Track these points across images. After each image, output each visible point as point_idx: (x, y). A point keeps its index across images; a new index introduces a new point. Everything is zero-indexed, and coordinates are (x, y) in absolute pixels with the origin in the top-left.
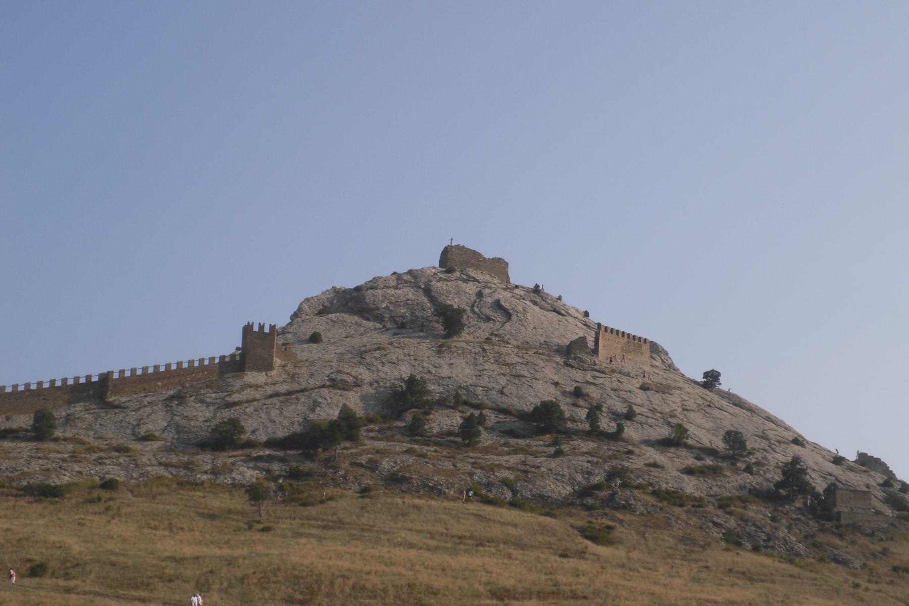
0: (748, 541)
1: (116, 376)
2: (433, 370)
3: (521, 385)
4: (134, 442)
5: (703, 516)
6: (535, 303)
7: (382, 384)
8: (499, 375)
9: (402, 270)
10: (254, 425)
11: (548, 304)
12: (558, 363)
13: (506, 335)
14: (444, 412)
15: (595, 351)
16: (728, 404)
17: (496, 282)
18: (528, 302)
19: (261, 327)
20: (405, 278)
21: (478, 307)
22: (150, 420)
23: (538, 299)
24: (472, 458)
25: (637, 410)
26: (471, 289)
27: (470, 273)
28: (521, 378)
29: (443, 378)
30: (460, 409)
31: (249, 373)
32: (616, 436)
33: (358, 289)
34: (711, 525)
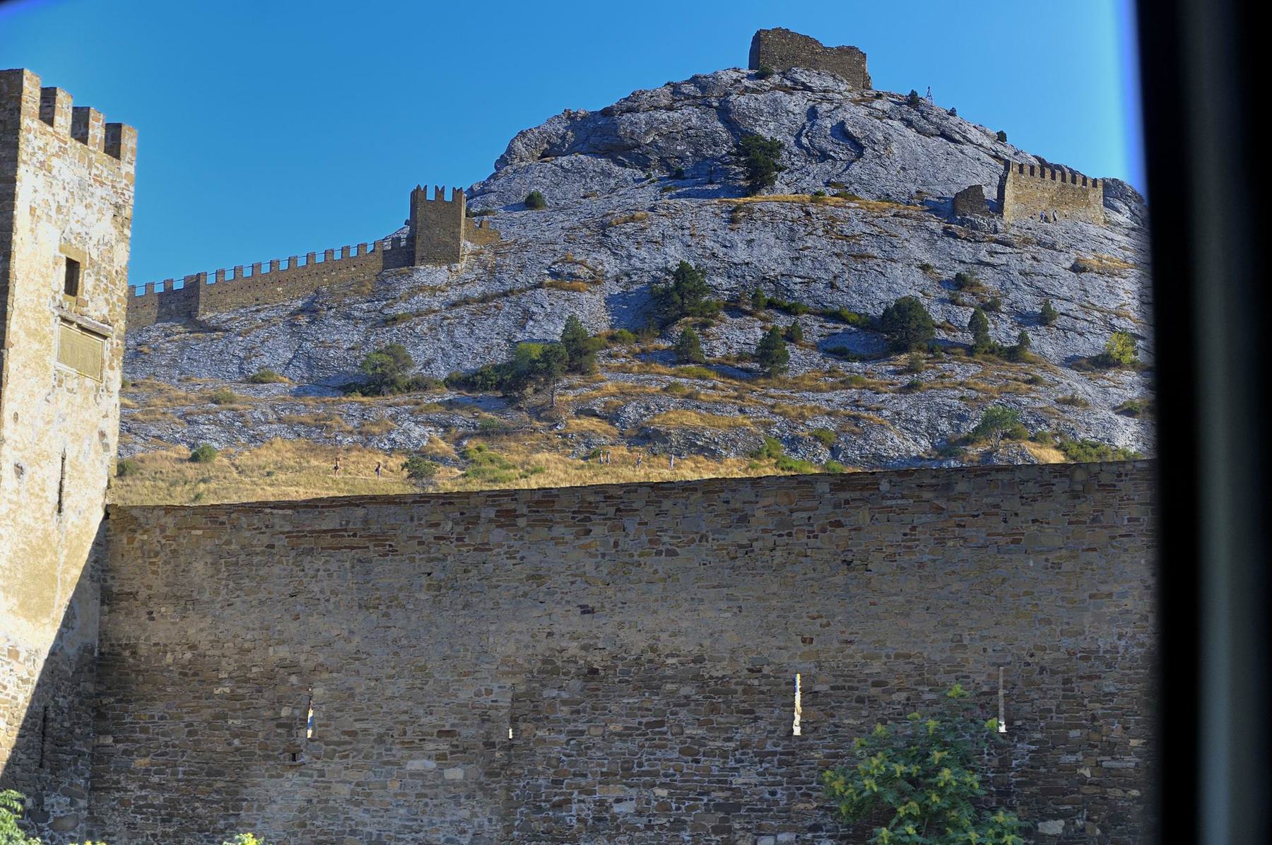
1: (211, 280)
2: (720, 252)
4: (243, 385)
6: (909, 124)
7: (635, 278)
11: (932, 123)
12: (932, 232)
13: (851, 184)
14: (735, 320)
15: (998, 207)
17: (842, 89)
18: (896, 123)
19: (440, 193)
23: (914, 116)
24: (772, 397)
25: (1059, 307)
26: (797, 104)
27: (797, 76)
28: (866, 260)
29: (735, 264)
30: (763, 314)
31: (422, 267)
32: (1013, 355)
33: (607, 112)
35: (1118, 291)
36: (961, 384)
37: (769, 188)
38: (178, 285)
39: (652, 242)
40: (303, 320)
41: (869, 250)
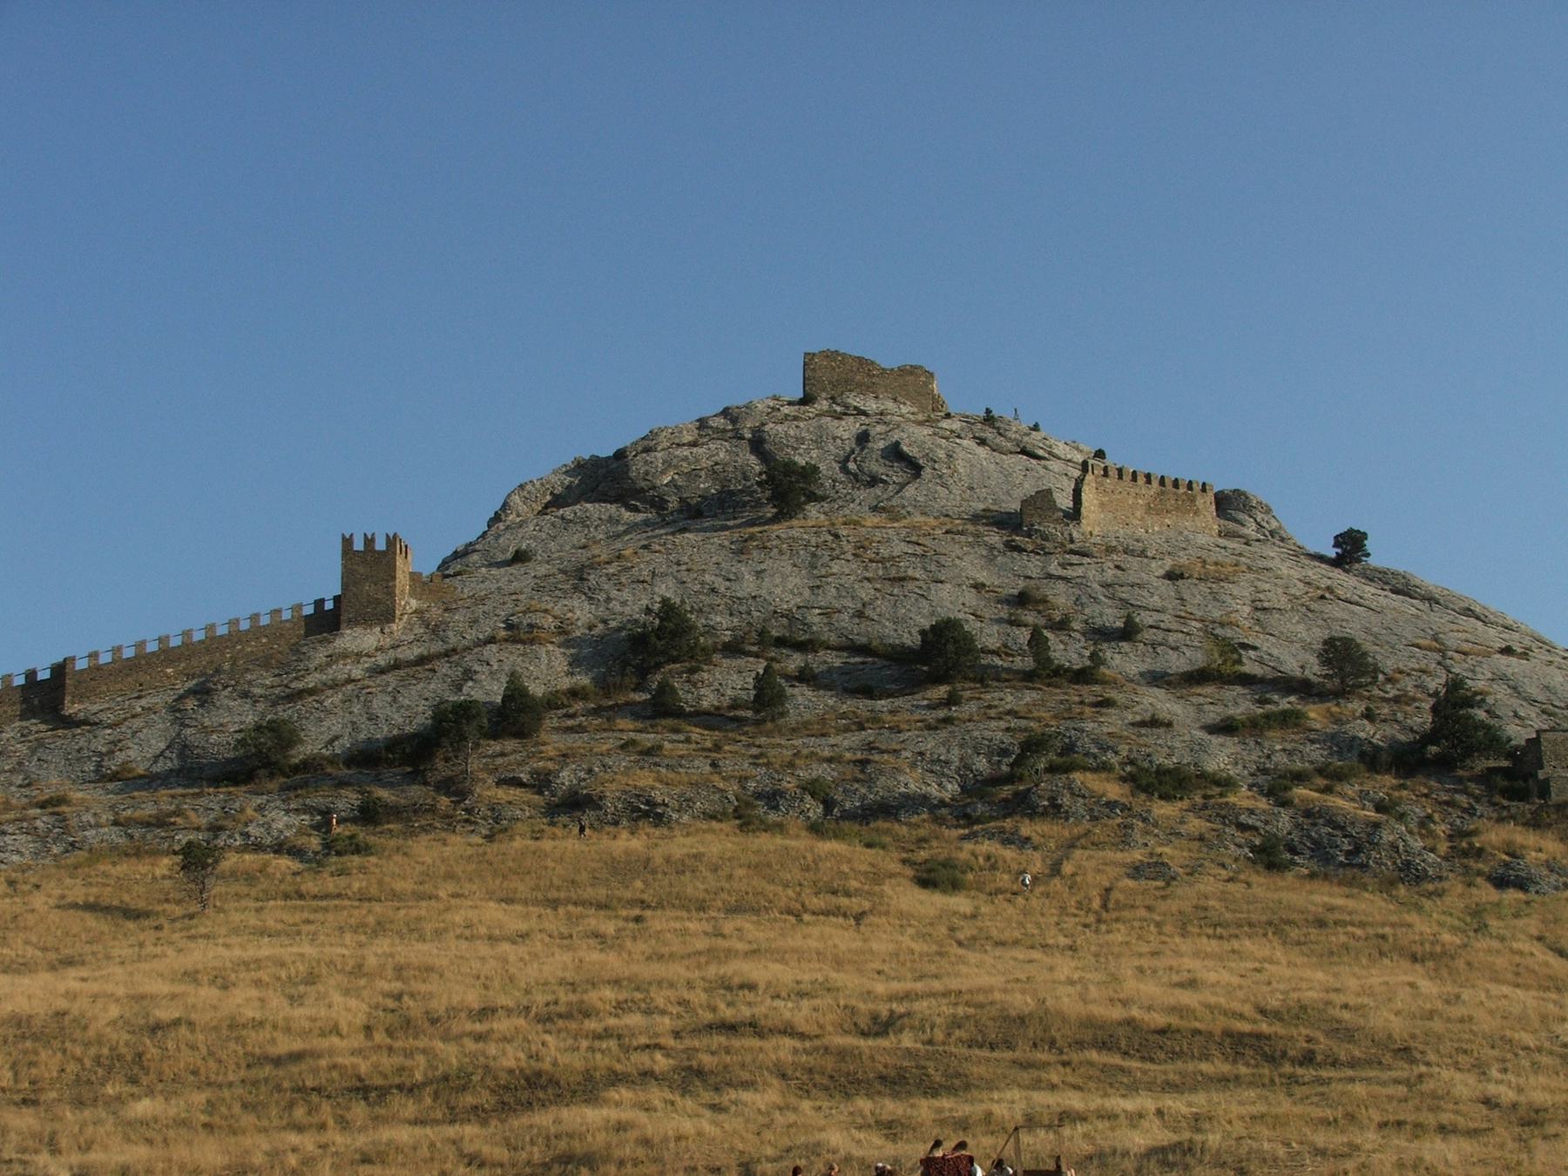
0: (1312, 857)
2: (721, 585)
5: (1218, 815)
6: (982, 442)
9: (710, 408)
10: (334, 728)
12: (992, 548)
15: (1075, 514)
16: (1380, 592)
19: (369, 541)
20: (714, 425)
21: (855, 461)
29: (739, 598)
31: (348, 632)
32: (1082, 676)
33: (620, 455)
35: (1224, 597)
36: (1009, 712)
37: (801, 516)
38: (44, 675)
39: (638, 581)
40: (190, 704)
41: (910, 572)
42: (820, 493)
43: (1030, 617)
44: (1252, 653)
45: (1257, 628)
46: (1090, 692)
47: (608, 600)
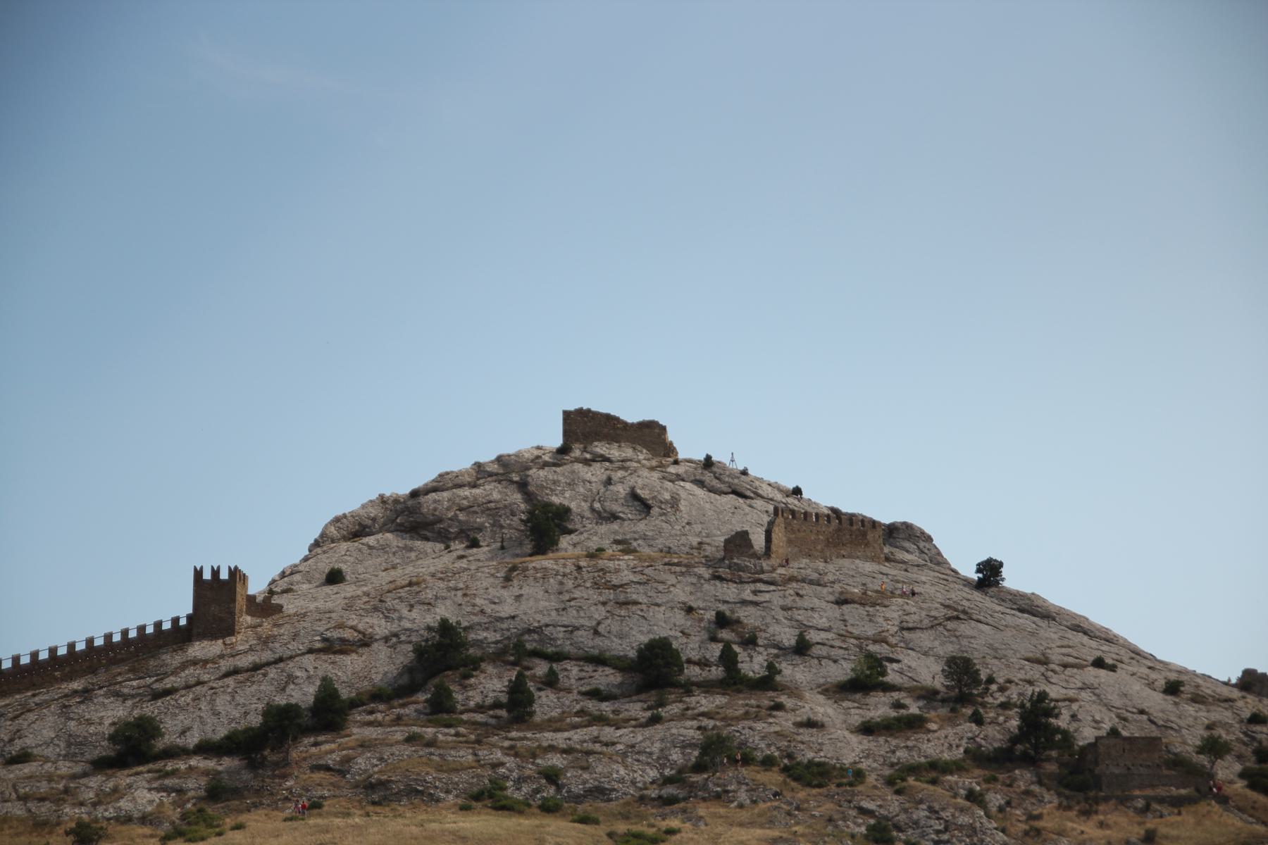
2: (489, 609)
3: (629, 617)
6: (700, 483)
8: (596, 605)
11: (724, 482)
12: (700, 577)
16: (1008, 611)
19: (215, 573)
21: (600, 501)
22: (31, 730)
26: (595, 473)
31: (198, 643)
33: (415, 494)
34: (853, 813)
36: (703, 714)
41: (634, 597)
42: (570, 527)
43: (725, 634)
44: (895, 666)
45: (902, 645)
46: (765, 699)
47: (400, 619)
